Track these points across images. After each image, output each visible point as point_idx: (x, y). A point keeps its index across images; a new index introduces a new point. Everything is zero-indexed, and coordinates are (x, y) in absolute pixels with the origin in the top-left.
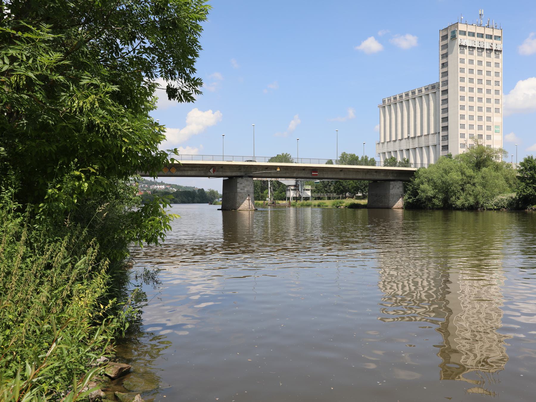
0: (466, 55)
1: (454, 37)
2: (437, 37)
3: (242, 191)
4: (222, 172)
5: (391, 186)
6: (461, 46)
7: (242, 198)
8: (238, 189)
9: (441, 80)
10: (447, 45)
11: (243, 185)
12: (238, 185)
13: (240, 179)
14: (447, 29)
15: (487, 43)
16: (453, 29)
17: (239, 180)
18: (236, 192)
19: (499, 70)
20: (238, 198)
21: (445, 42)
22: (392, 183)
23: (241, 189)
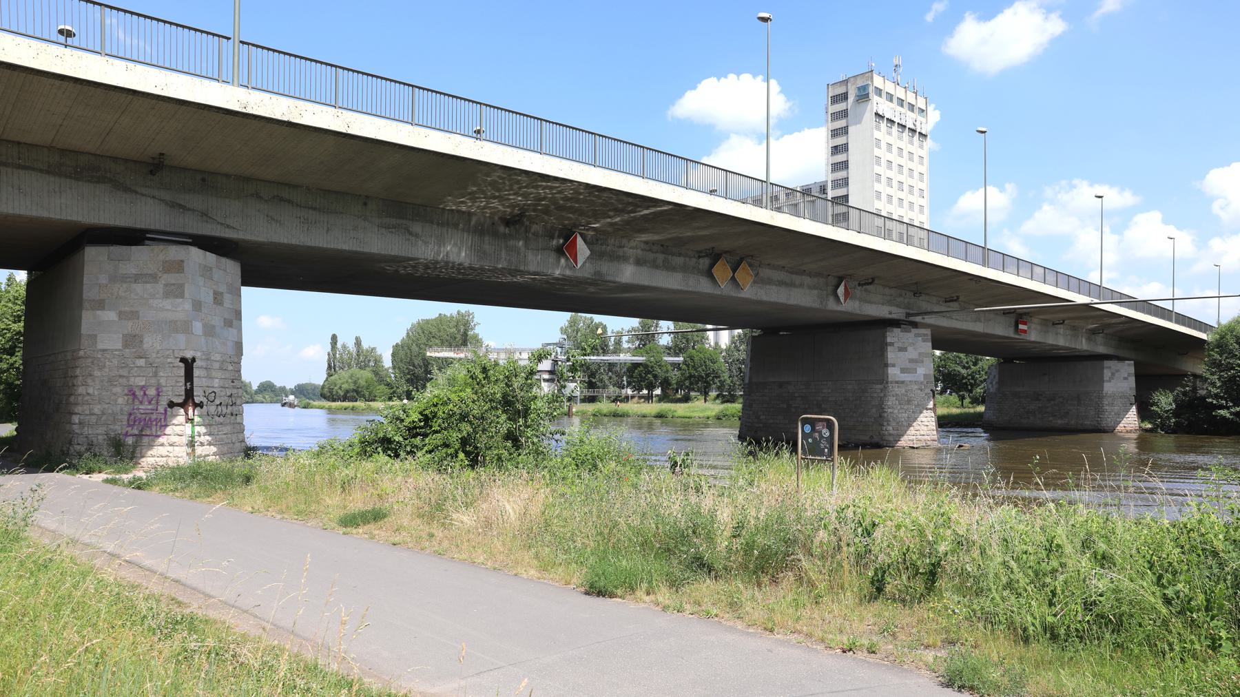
0: (883, 133)
1: (863, 96)
2: (823, 98)
3: (906, 377)
4: (861, 300)
5: (1107, 374)
6: (877, 114)
7: (909, 402)
8: (891, 371)
9: (831, 177)
10: (844, 114)
11: (912, 353)
12: (891, 355)
13: (897, 331)
14: (846, 82)
15: (909, 119)
16: (860, 83)
17: (893, 336)
18: (883, 380)
19: (923, 169)
20: (891, 401)
21: (840, 107)
22: (1107, 363)
23: (903, 371)
